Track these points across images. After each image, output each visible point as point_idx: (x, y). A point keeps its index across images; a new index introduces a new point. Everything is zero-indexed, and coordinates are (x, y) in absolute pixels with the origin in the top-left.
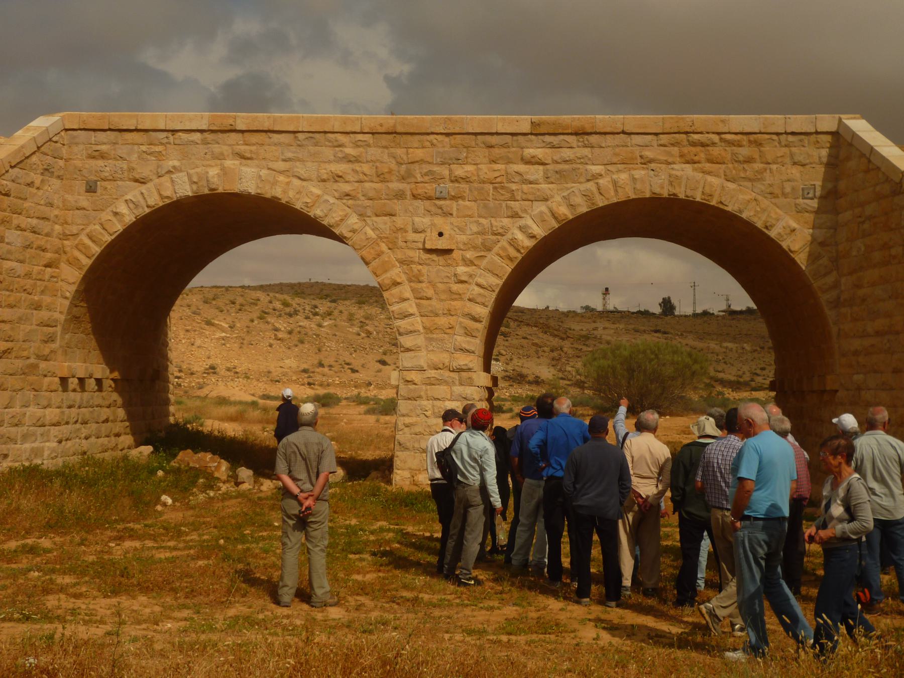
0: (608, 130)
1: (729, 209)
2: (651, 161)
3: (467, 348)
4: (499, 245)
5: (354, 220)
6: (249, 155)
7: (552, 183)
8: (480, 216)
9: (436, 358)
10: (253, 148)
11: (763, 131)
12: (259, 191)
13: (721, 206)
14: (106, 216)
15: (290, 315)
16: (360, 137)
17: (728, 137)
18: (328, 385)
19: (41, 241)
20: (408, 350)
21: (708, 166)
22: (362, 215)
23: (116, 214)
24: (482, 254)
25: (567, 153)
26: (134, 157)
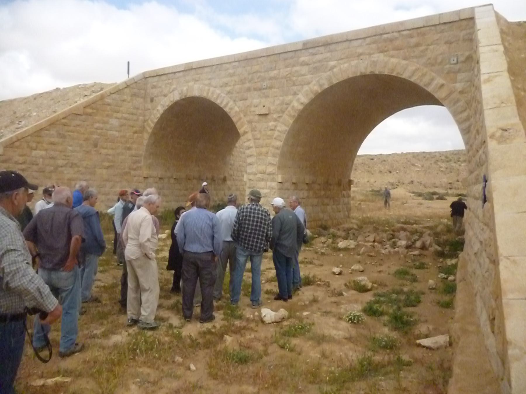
0: (340, 40)
1: (403, 77)
2: (361, 54)
3: (273, 163)
4: (288, 109)
5: (231, 103)
6: (197, 79)
7: (312, 74)
8: (280, 96)
9: (262, 168)
10: (198, 76)
11: (425, 25)
12: (199, 95)
13: (399, 76)
14: (155, 112)
15: (448, 162)
16: (234, 64)
17: (405, 33)
18: (458, 189)
19: (131, 123)
20: (250, 164)
21: (391, 53)
22: (235, 101)
23: (158, 110)
24: (281, 115)
25: (319, 57)
26: (163, 86)
